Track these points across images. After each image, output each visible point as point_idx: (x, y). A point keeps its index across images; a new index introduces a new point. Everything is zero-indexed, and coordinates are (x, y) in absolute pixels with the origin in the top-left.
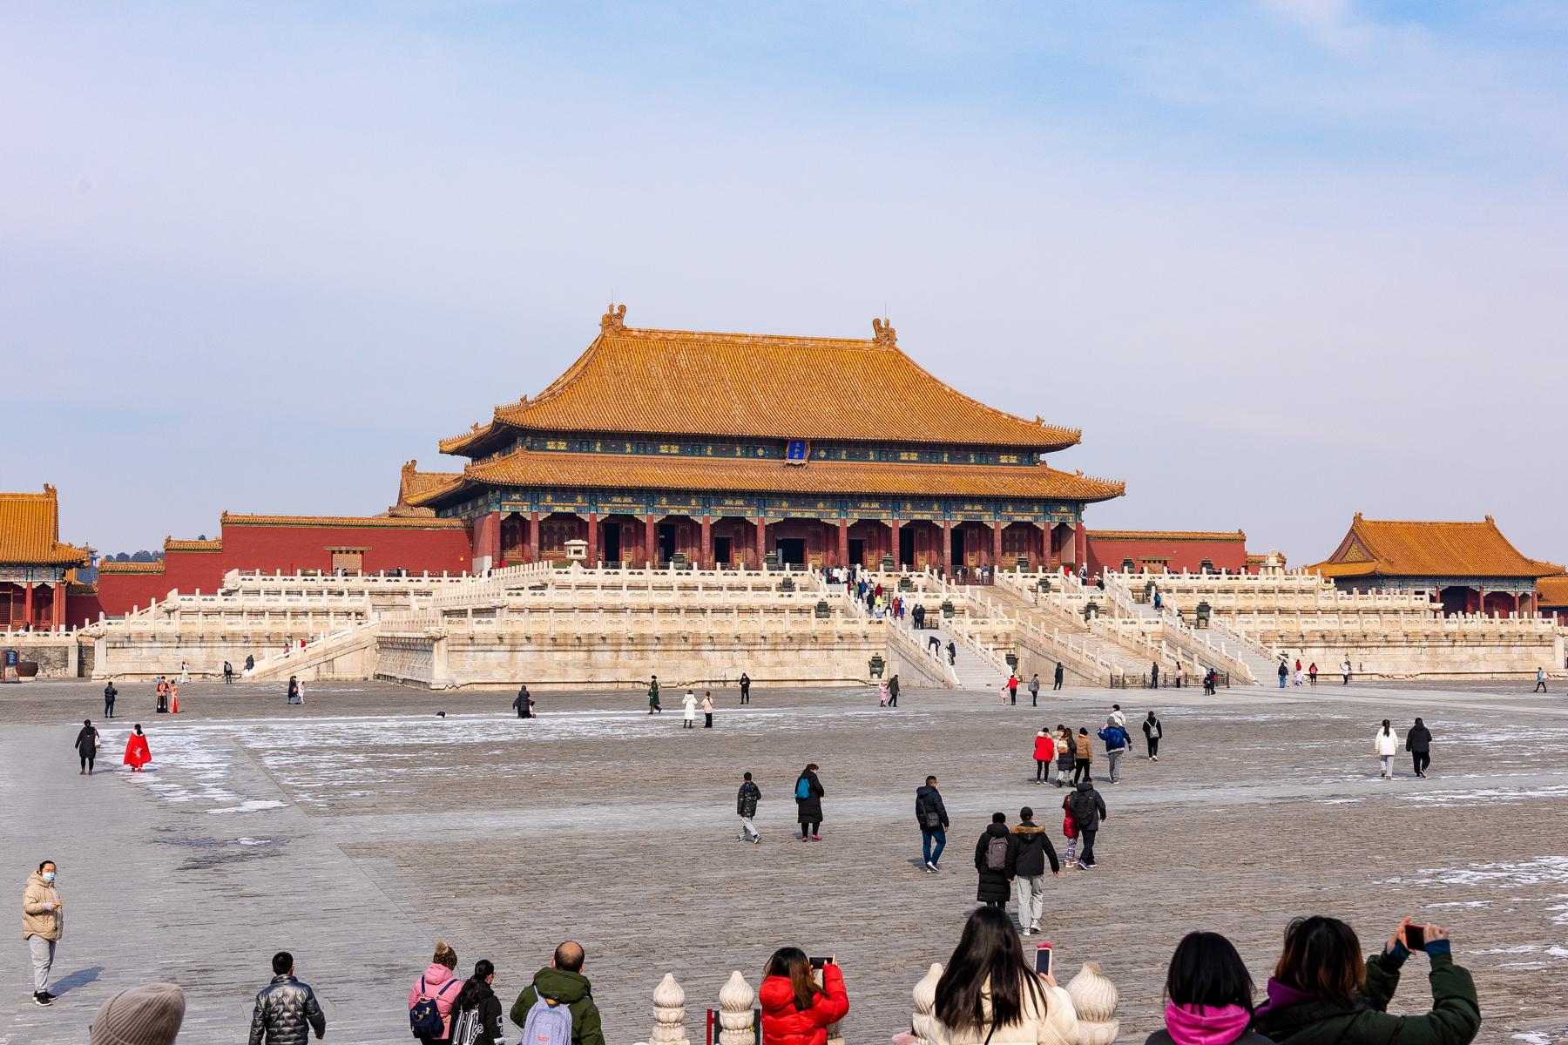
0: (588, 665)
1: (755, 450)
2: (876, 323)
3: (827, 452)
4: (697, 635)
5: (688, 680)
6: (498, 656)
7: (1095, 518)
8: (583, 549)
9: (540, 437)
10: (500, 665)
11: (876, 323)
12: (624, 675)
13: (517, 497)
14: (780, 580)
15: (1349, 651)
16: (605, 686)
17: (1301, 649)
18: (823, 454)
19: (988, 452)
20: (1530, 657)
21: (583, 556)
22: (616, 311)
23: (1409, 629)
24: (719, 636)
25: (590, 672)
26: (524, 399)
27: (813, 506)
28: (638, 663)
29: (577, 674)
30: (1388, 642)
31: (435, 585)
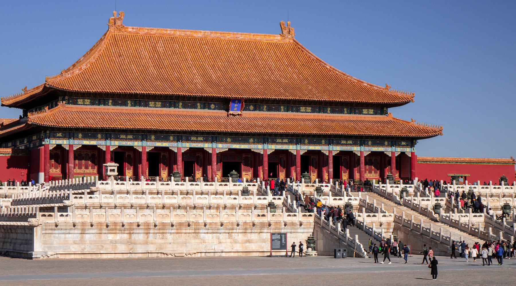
0: (130, 242)
4: (197, 224)
5: (191, 252)
6: (74, 236)
7: (423, 151)
8: (116, 168)
9: (73, 97)
10: (75, 243)
12: (151, 248)
13: (60, 135)
14: (241, 188)
16: (140, 256)
19: (355, 107)
24: (211, 224)
25: (131, 246)
27: (246, 141)
28: (160, 241)
29: (122, 248)
31: (12, 191)
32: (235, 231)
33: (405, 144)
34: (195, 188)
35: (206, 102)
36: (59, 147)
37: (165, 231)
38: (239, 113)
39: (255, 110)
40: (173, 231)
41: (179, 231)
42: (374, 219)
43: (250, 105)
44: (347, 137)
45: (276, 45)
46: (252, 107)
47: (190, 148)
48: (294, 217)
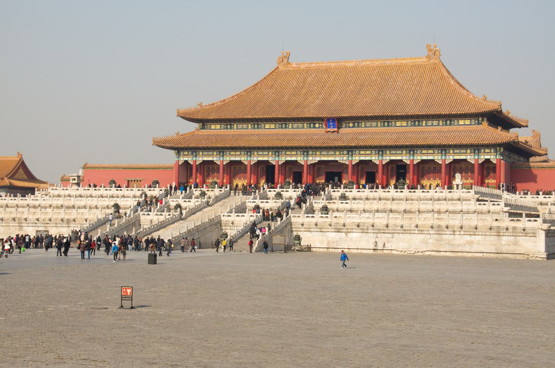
1: (314, 124)
2: (428, 46)
3: (354, 123)
4: (20, 219)
8: (76, 178)
11: (428, 46)
13: (186, 153)
15: (379, 235)
17: (346, 233)
18: (351, 125)
20: (516, 244)
21: (76, 181)
22: (285, 55)
23: (420, 223)
26: (200, 105)
30: (403, 230)
32: (48, 225)
33: (489, 151)
34: (120, 193)
35: (312, 120)
36: (186, 162)
37: (441, 232)
38: (336, 129)
39: (354, 127)
40: (3, 224)
41: (8, 225)
42: (312, 219)
43: (349, 123)
44: (429, 147)
45: (419, 67)
46: (351, 125)
47: (286, 161)
48: (243, 217)
